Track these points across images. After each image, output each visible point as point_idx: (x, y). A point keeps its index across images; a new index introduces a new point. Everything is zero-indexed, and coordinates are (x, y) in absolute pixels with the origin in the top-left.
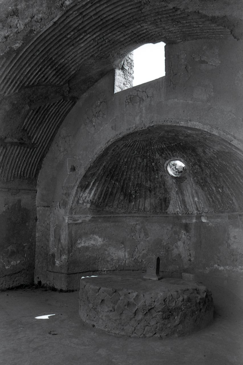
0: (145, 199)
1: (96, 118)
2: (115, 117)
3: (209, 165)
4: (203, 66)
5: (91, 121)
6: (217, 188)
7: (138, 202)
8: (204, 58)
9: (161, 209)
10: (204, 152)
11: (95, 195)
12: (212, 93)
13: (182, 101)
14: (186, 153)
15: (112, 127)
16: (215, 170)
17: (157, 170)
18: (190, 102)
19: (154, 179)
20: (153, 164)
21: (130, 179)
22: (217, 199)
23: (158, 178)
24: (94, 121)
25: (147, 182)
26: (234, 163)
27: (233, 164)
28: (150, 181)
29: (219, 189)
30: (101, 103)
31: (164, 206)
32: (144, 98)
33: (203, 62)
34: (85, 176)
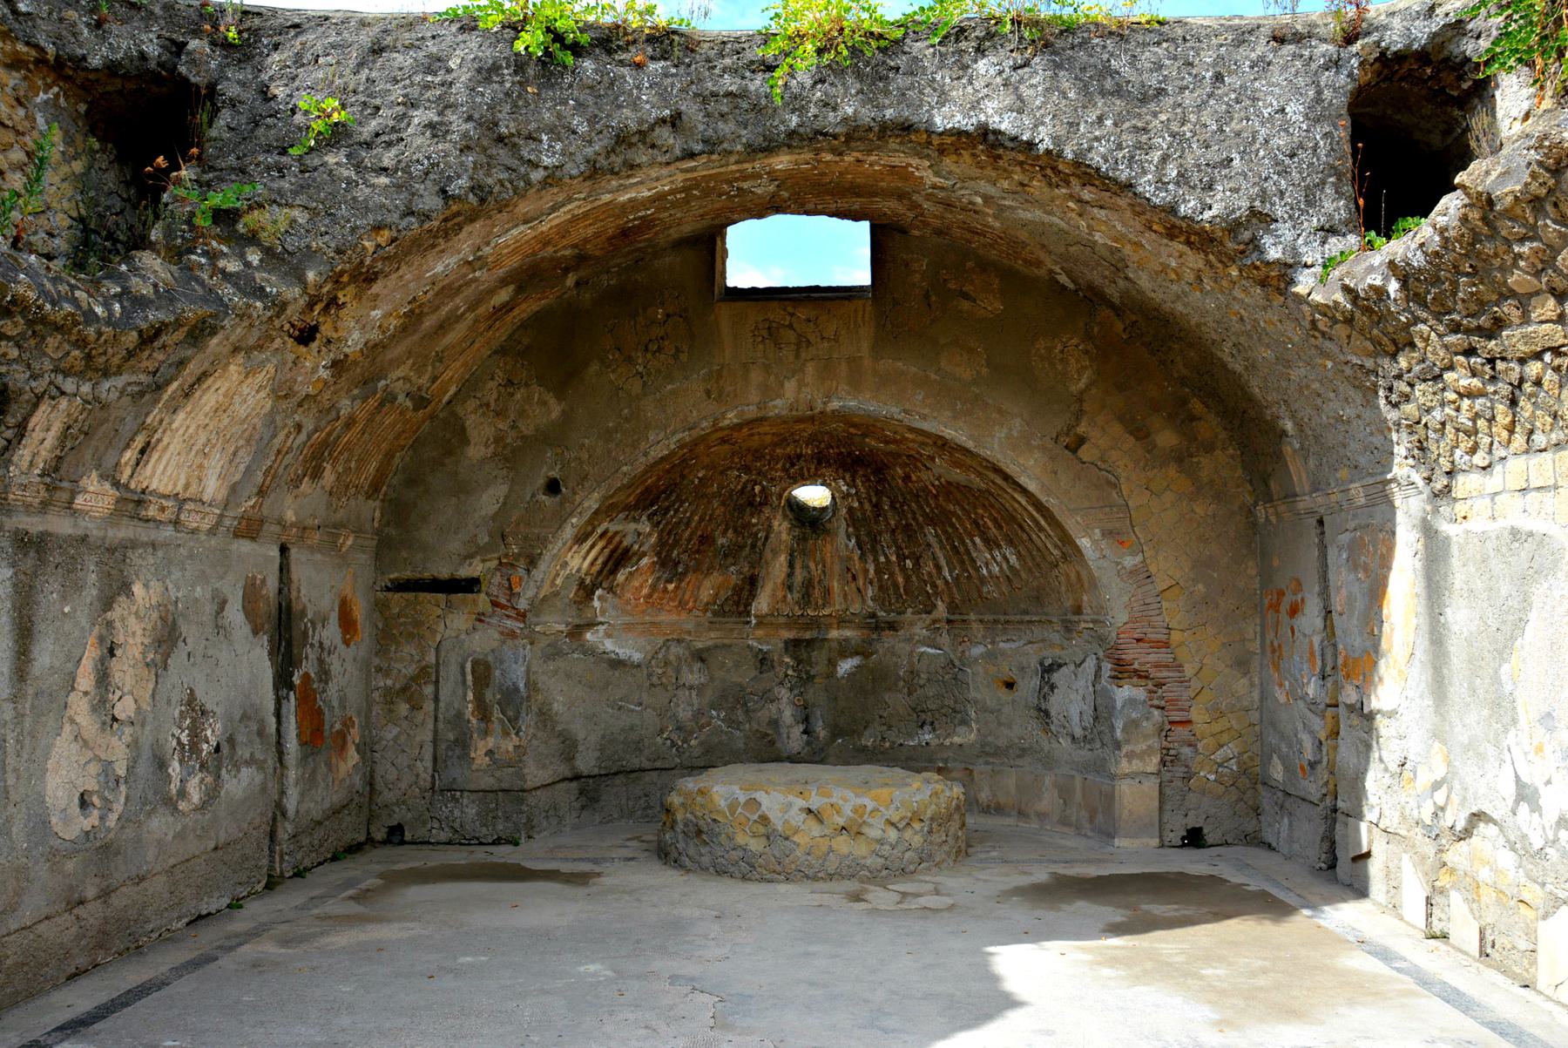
0: (708, 574)
1: (649, 356)
2: (716, 368)
3: (902, 506)
4: (966, 305)
5: (630, 360)
6: (902, 558)
7: (683, 585)
8: (967, 288)
9: (737, 603)
10: (907, 478)
11: (592, 564)
12: (985, 371)
13: (913, 369)
14: (856, 472)
15: (708, 393)
16: (914, 519)
17: (760, 504)
18: (933, 376)
19: (748, 525)
20: (757, 488)
21: (688, 525)
22: (896, 586)
23: (754, 525)
24: (640, 361)
25: (724, 533)
26: (980, 511)
27: (976, 513)
28: (735, 531)
29: (908, 561)
30: (668, 316)
31: (745, 593)
32: (812, 338)
33: (966, 296)
34: (596, 513)
